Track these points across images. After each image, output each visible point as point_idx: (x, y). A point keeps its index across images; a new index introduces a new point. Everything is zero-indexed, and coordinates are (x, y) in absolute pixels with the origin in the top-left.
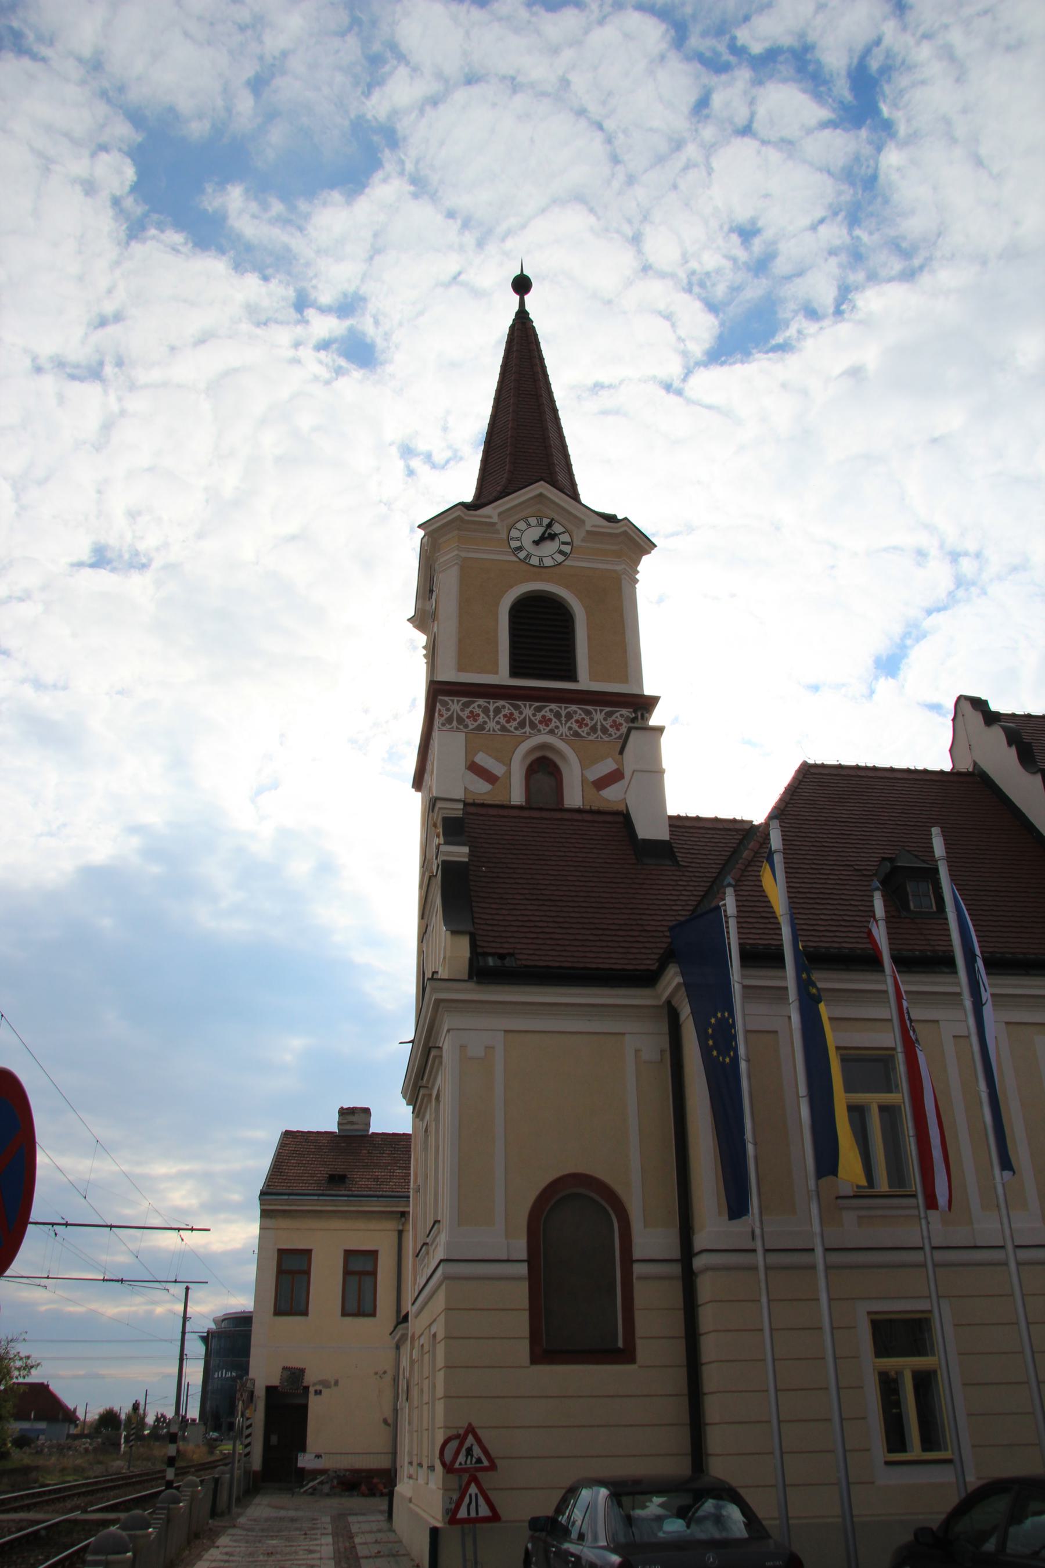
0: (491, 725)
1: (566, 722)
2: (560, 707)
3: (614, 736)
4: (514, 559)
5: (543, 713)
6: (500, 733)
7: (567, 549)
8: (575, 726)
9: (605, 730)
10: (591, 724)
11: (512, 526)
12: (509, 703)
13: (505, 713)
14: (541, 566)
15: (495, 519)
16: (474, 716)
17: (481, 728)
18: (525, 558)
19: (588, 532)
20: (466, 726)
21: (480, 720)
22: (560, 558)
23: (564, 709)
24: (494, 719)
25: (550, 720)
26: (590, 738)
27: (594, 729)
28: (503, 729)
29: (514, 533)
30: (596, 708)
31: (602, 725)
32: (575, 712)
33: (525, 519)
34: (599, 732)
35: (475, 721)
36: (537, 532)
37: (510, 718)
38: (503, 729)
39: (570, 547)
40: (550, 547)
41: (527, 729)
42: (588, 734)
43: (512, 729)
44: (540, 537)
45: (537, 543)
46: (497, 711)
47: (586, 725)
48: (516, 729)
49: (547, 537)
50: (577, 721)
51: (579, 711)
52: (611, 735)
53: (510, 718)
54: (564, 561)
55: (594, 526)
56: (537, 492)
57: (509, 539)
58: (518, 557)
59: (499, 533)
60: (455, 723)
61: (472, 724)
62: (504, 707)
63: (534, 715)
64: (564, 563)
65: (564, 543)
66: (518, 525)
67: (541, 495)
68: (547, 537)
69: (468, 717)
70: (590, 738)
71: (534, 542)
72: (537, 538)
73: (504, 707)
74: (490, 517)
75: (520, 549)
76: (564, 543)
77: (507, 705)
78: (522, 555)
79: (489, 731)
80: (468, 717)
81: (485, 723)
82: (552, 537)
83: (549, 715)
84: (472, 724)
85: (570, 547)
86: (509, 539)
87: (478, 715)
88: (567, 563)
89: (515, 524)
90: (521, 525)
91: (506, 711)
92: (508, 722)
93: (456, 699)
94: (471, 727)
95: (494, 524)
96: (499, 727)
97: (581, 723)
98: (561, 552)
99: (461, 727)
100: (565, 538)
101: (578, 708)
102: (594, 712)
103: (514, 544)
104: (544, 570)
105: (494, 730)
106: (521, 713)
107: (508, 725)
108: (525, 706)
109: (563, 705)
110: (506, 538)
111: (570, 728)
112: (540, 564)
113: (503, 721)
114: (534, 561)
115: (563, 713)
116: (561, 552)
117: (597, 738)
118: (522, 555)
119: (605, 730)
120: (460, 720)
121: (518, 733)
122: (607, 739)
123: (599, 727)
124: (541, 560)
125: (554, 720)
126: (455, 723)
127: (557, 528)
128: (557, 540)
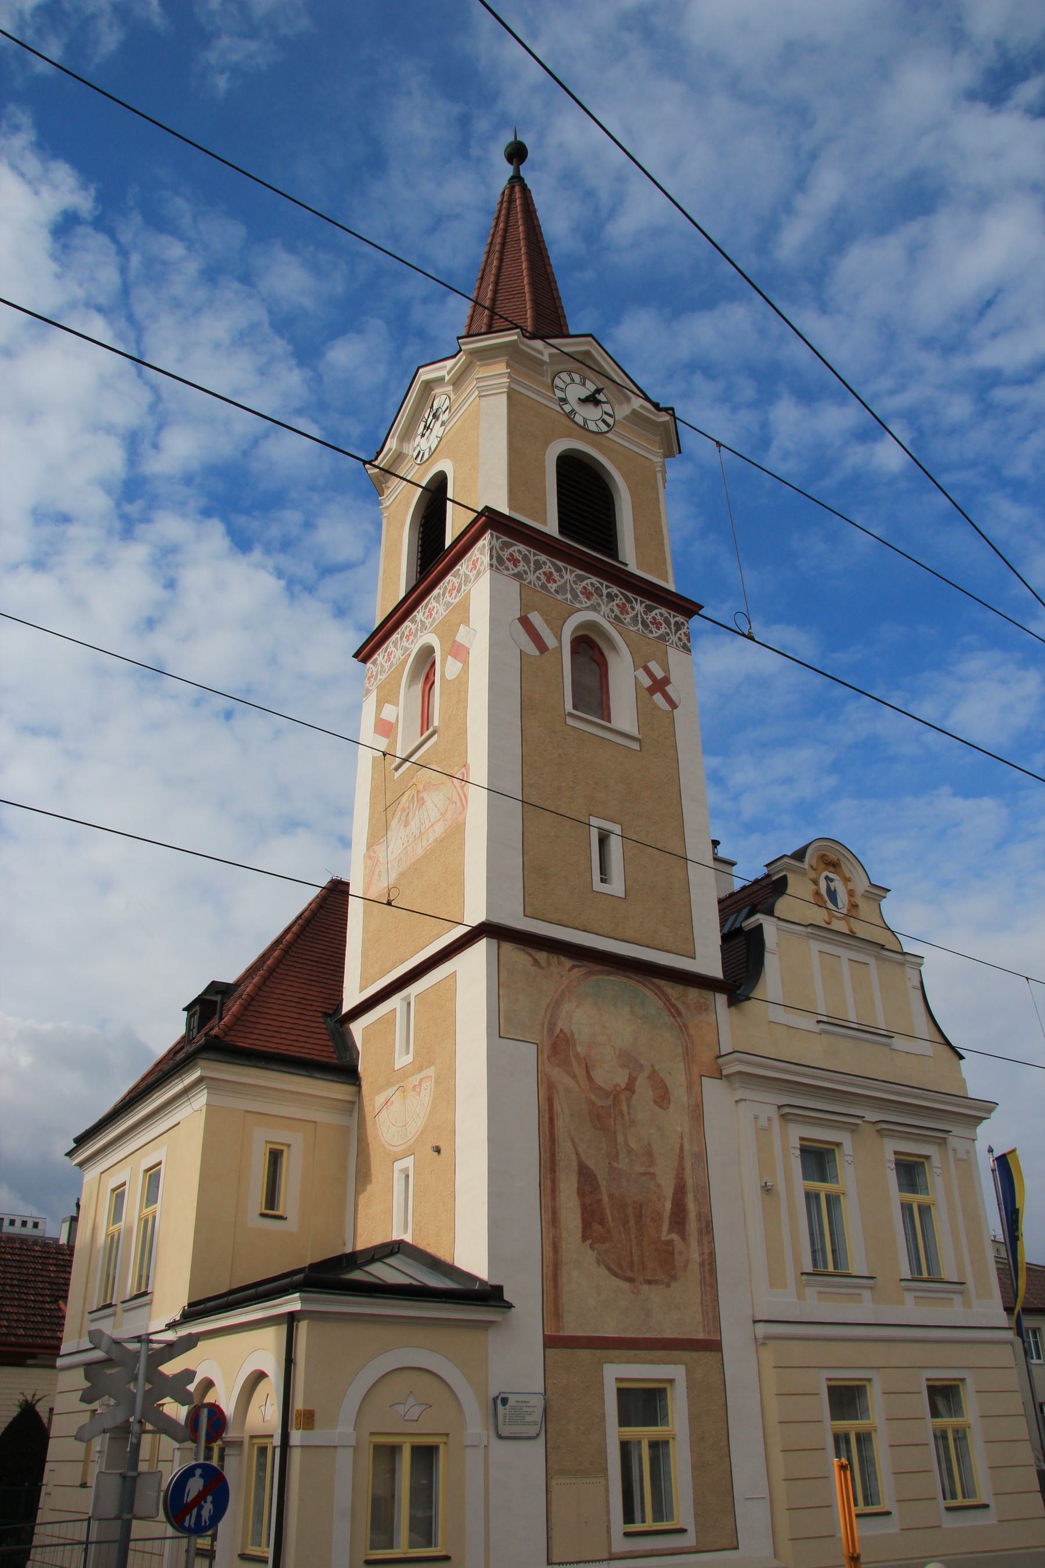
0: (531, 577)
1: (608, 603)
4: (559, 409)
6: (540, 590)
11: (556, 374)
13: (545, 570)
14: (584, 428)
15: (546, 359)
19: (634, 410)
22: (605, 428)
27: (635, 619)
28: (544, 587)
29: (558, 382)
30: (636, 596)
34: (640, 625)
36: (584, 393)
44: (587, 397)
49: (592, 400)
54: (607, 432)
57: (553, 387)
58: (562, 409)
59: (542, 376)
62: (545, 563)
66: (561, 375)
67: (588, 353)
68: (592, 400)
70: (631, 628)
71: (579, 399)
72: (583, 397)
74: (541, 353)
75: (564, 401)
79: (530, 583)
82: (597, 403)
86: (553, 387)
88: (609, 435)
89: (561, 372)
92: (549, 582)
95: (542, 363)
97: (623, 609)
101: (619, 591)
102: (634, 601)
103: (559, 394)
104: (587, 434)
109: (605, 583)
112: (584, 425)
114: (579, 420)
116: (604, 421)
117: (638, 630)
118: (567, 408)
119: (645, 624)
124: (585, 420)
127: (601, 397)
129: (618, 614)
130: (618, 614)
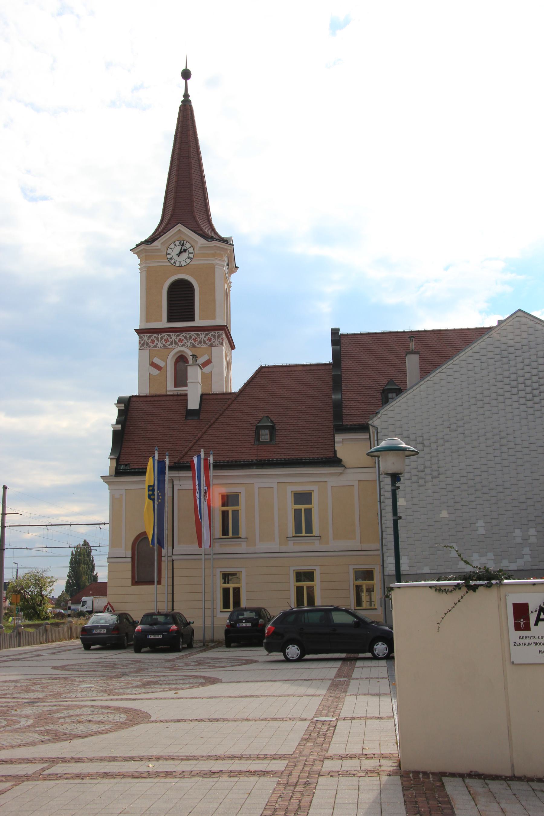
0: (160, 345)
2: (187, 334)
3: (208, 344)
5: (180, 337)
7: (191, 255)
8: (193, 342)
9: (205, 342)
10: (199, 340)
11: (168, 247)
12: (168, 335)
15: (159, 247)
16: (153, 342)
17: (155, 346)
18: (174, 263)
19: (200, 247)
20: (150, 347)
21: (155, 343)
22: (188, 261)
23: (188, 335)
24: (161, 341)
25: (183, 340)
26: (199, 346)
27: (200, 342)
28: (164, 346)
29: (169, 251)
31: (204, 340)
32: (193, 335)
33: (174, 243)
35: (153, 343)
37: (167, 341)
38: (164, 346)
39: (193, 254)
40: (184, 255)
41: (174, 345)
42: (198, 344)
43: (168, 346)
45: (178, 255)
46: (162, 338)
47: (197, 340)
48: (169, 345)
50: (193, 339)
51: (194, 335)
52: (207, 344)
53: (167, 341)
55: (202, 244)
56: (178, 229)
60: (145, 346)
61: (152, 345)
62: (164, 336)
63: (176, 338)
64: (190, 263)
65: (190, 253)
66: (170, 247)
69: (150, 342)
70: (199, 346)
72: (178, 253)
73: (164, 336)
75: (172, 258)
76: (190, 253)
77: (166, 335)
78: (172, 262)
80: (150, 342)
81: (157, 344)
82: (185, 251)
83: (182, 338)
84: (152, 345)
85: (193, 254)
86: (167, 254)
87: (154, 341)
90: (172, 246)
91: (165, 338)
93: (145, 335)
94: (152, 347)
96: (162, 345)
97: (195, 340)
98: (189, 258)
99: (148, 347)
100: (191, 250)
104: (183, 268)
105: (161, 347)
106: (171, 338)
107: (166, 344)
108: (173, 335)
110: (166, 254)
111: (191, 343)
113: (164, 342)
115: (188, 336)
116: (189, 258)
118: (172, 262)
119: (205, 342)
120: (147, 344)
121: (170, 347)
122: (205, 346)
123: (202, 341)
125: (184, 340)
126: (145, 346)
127: (188, 245)
128: (187, 251)
129: (193, 343)
130: (193, 343)
